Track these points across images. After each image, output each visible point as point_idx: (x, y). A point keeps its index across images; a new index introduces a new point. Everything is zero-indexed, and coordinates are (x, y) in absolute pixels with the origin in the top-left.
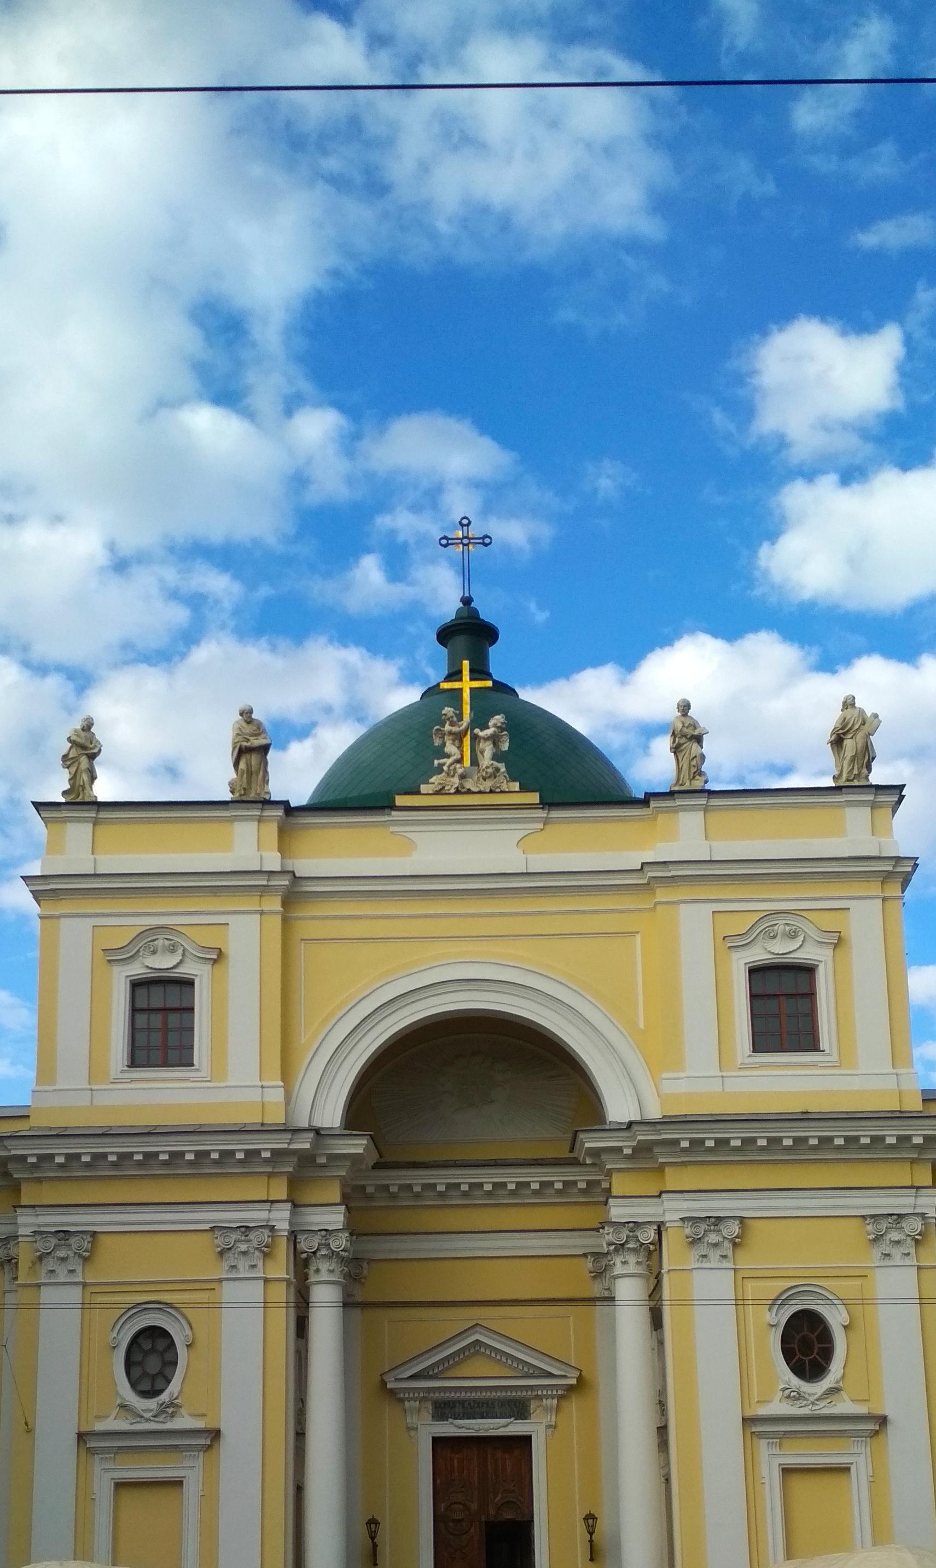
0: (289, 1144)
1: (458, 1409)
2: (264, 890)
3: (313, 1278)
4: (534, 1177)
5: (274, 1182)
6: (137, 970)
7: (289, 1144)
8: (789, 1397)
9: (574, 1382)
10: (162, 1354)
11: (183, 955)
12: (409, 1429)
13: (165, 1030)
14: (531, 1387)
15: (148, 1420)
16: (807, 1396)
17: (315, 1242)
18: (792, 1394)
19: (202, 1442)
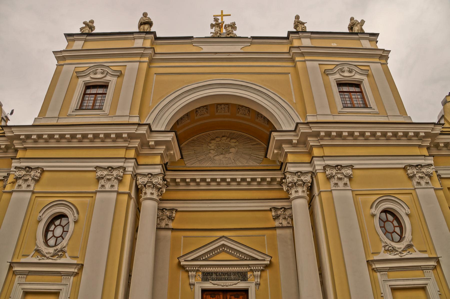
0: (136, 131)
1: (214, 276)
2: (142, 55)
3: (143, 196)
4: (249, 176)
5: (128, 152)
6: (87, 79)
7: (136, 131)
8: (388, 250)
9: (267, 262)
10: (63, 227)
11: (107, 74)
12: (190, 284)
13: (95, 101)
14: (248, 265)
15: (48, 258)
16: (397, 249)
17: (146, 180)
18: (390, 248)
19: (72, 270)
